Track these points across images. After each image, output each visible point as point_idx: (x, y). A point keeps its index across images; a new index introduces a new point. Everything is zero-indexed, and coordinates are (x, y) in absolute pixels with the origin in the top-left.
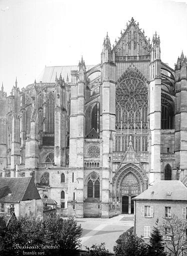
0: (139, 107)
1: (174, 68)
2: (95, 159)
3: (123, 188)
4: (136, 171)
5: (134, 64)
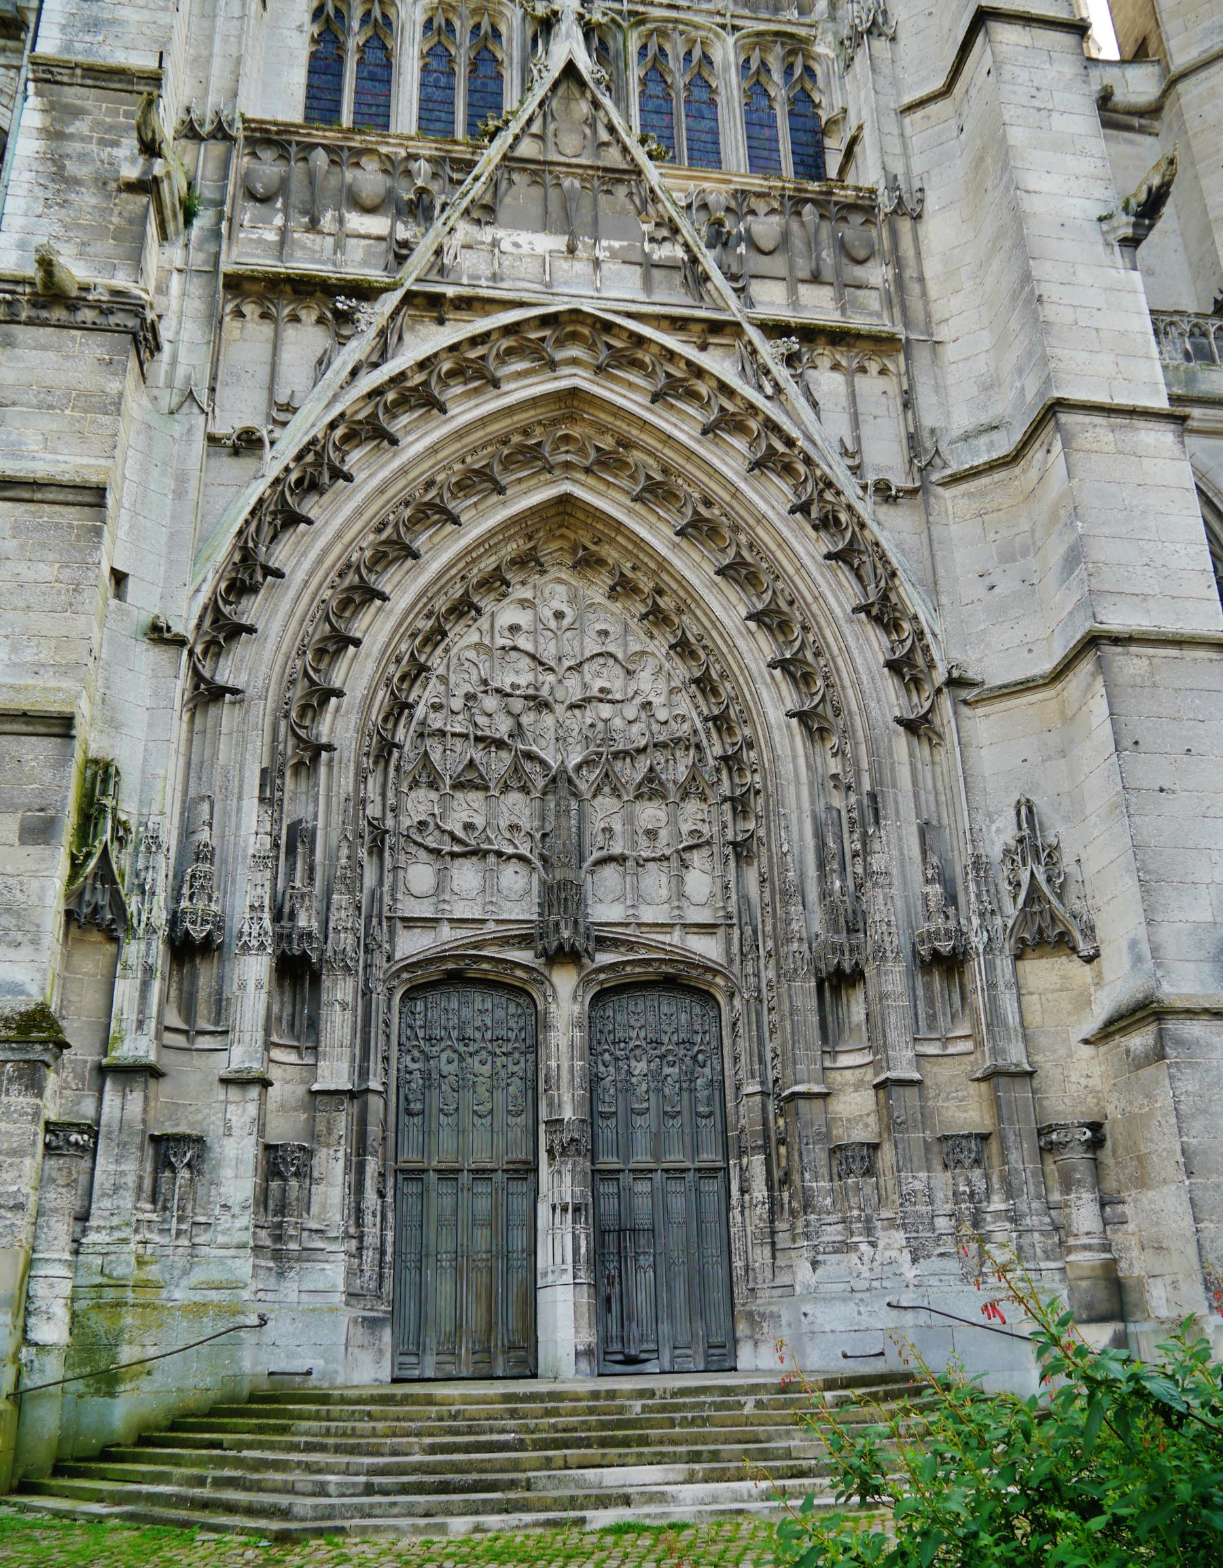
3: (420, 804)
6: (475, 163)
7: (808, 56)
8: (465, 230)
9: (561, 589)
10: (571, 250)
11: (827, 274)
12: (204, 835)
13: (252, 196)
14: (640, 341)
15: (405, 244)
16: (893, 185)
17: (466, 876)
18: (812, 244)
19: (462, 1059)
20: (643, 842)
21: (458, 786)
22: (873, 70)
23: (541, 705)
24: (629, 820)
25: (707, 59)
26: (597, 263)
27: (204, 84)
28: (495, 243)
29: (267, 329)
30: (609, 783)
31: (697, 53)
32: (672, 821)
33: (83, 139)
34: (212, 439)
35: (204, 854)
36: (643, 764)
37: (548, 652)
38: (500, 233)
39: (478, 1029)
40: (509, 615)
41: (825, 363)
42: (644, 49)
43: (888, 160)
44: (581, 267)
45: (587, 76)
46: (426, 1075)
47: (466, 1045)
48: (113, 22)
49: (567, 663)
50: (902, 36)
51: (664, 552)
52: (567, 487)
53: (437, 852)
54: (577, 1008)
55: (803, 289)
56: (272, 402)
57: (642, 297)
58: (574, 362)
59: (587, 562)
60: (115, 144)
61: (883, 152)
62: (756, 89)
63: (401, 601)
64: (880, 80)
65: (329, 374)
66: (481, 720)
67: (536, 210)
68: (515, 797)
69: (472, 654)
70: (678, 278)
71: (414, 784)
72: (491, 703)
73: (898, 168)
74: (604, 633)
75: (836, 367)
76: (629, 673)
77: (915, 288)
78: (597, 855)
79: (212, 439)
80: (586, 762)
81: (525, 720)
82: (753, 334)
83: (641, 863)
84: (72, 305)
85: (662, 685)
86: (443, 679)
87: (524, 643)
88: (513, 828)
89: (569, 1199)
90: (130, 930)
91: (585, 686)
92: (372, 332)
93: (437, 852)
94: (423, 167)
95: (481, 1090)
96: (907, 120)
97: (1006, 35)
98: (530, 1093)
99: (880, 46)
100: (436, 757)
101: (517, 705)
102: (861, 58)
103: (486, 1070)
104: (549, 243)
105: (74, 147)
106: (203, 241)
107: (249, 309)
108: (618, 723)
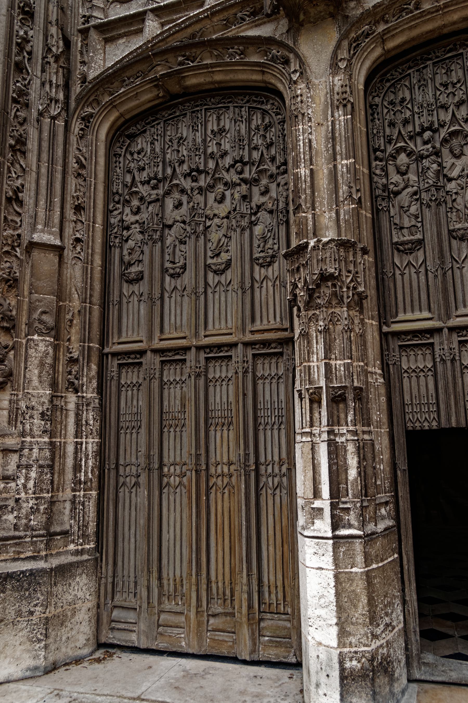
19: (190, 198)
39: (212, 156)
47: (195, 180)
54: (338, 80)
89: (322, 383)
95: (215, 236)
98: (283, 229)
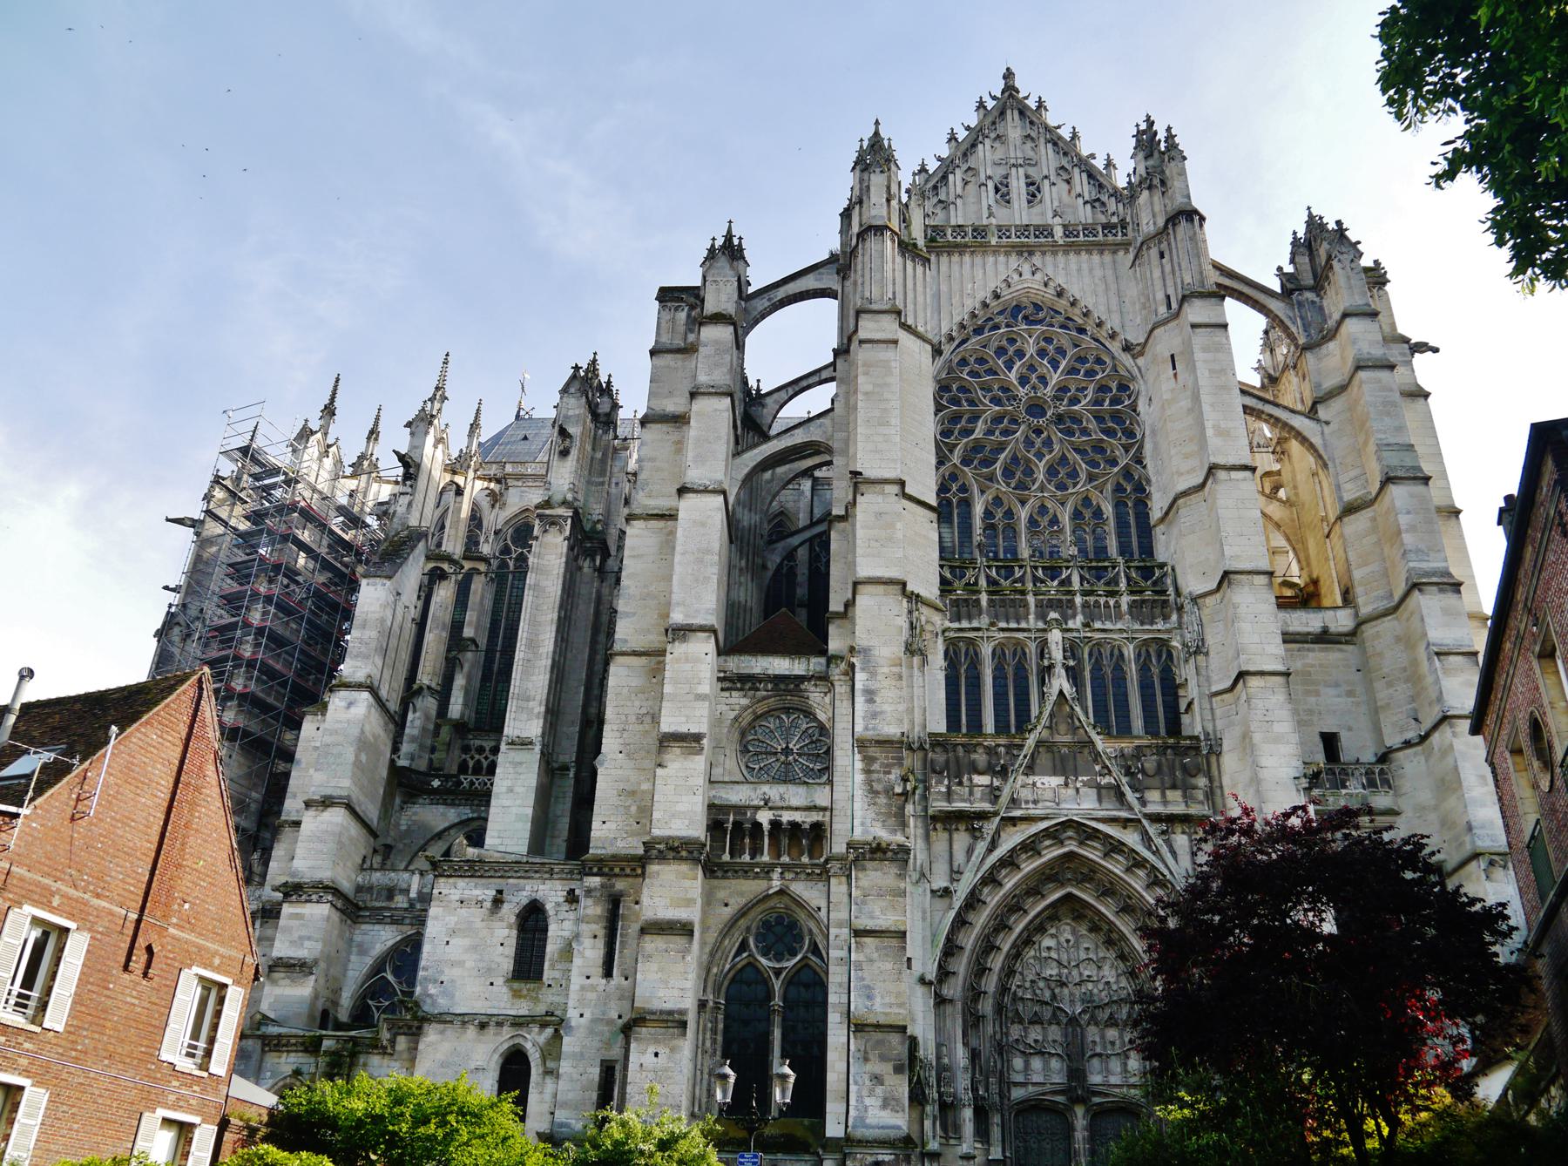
0: (1091, 478)
1: (1275, 285)
2: (796, 795)
3: (1015, 1031)
4: (1109, 889)
5: (1037, 260)
6: (1023, 746)
7: (1168, 646)
8: (1021, 779)
9: (1068, 928)
10: (1066, 785)
11: (1179, 783)
12: (946, 1060)
13: (934, 771)
14: (1097, 830)
15: (998, 789)
16: (1207, 734)
17: (1036, 1063)
18: (1172, 769)
20: (1109, 1046)
21: (1031, 1023)
22: (1197, 674)
23: (1063, 984)
24: (1103, 1037)
25: (1121, 655)
26: (1077, 790)
27: (912, 722)
28: (1034, 784)
29: (946, 835)
30: (1093, 1020)
31: (1116, 652)
32: (1121, 1037)
33: (879, 772)
34: (932, 891)
35: (946, 1068)
36: (1108, 1011)
37: (1064, 958)
38: (1036, 778)
40: (1048, 942)
41: (1180, 830)
42: (1090, 655)
43: (1205, 723)
44: (1071, 792)
45: (1068, 697)
46: (1026, 1148)
48: (881, 712)
49: (1073, 964)
50: (1212, 653)
51: (1112, 918)
52: (1070, 889)
53: (1024, 1053)
55: (1168, 792)
56: (952, 870)
57: (1097, 805)
58: (1070, 838)
59: (1078, 917)
60: (889, 773)
61: (1202, 720)
62: (1144, 669)
63: (1006, 947)
64: (1201, 678)
65: (973, 858)
66: (1038, 992)
67: (1050, 764)
68: (1054, 1027)
69: (1032, 961)
70: (1112, 793)
71: (1013, 1022)
72: (1041, 984)
73: (1210, 729)
74: (1087, 949)
75: (1183, 833)
76: (1099, 967)
77: (1218, 792)
78: (1090, 1053)
79: (932, 891)
80: (1084, 1011)
81: (1057, 991)
82: (1145, 822)
83: (1108, 1056)
84: (884, 851)
85: (1114, 972)
86: (1021, 974)
87: (1054, 955)
88: (1055, 1041)
90: (927, 1102)
91: (1081, 974)
92: (989, 839)
93: (1024, 1053)
94: (1002, 750)
96: (1214, 699)
97: (1254, 682)
99: (1201, 658)
100: (1020, 1009)
101: (1053, 985)
102: (1192, 660)
103: (1049, 1146)
104: (1056, 781)
105: (875, 776)
106: (920, 800)
107: (939, 826)
108: (1095, 991)
